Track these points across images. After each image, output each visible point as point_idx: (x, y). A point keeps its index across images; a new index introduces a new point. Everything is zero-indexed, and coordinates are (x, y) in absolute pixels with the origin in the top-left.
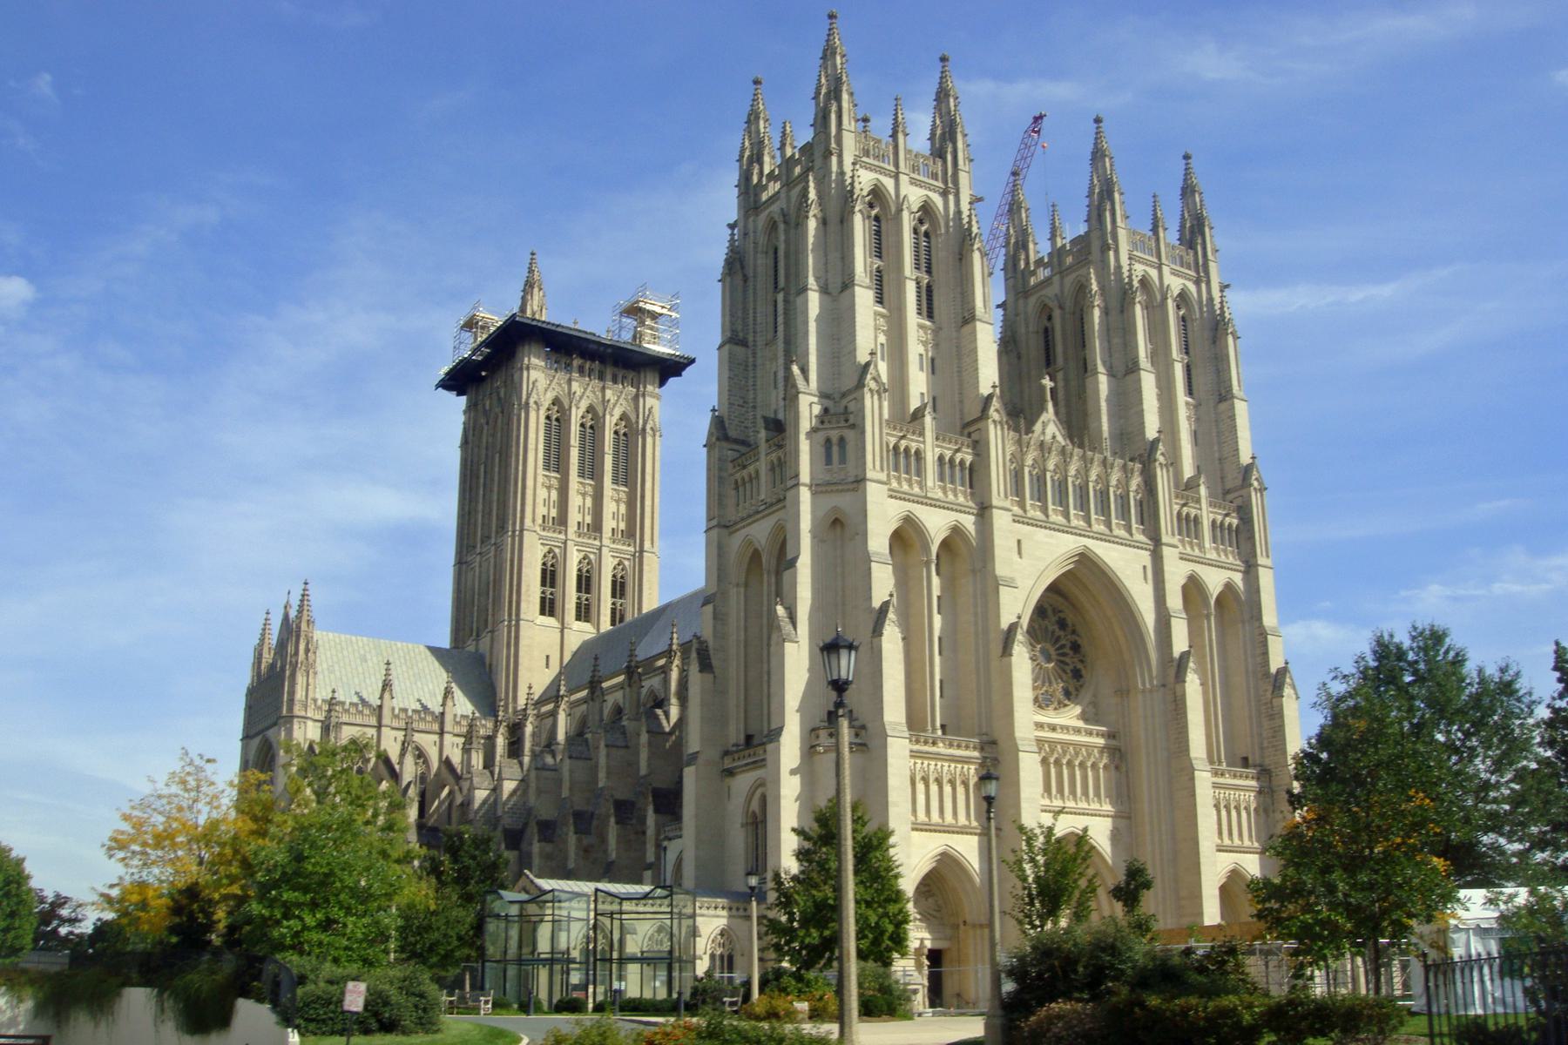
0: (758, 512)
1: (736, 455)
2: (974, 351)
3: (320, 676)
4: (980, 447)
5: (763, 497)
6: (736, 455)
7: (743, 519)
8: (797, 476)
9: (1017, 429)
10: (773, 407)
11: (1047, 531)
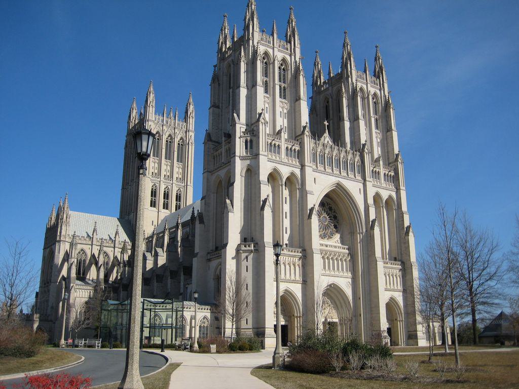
0: (221, 166)
1: (214, 146)
2: (300, 111)
4: (302, 145)
5: (223, 161)
6: (214, 146)
7: (216, 169)
8: (235, 153)
9: (314, 139)
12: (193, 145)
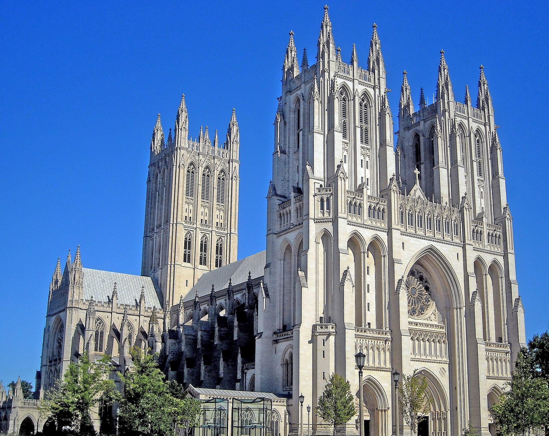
0: (290, 228)
3: (84, 289)
6: (280, 202)
7: (283, 231)
8: (308, 214)
10: (297, 181)
11: (415, 239)
12: (238, 179)
